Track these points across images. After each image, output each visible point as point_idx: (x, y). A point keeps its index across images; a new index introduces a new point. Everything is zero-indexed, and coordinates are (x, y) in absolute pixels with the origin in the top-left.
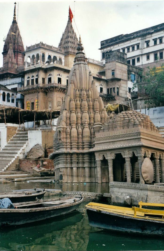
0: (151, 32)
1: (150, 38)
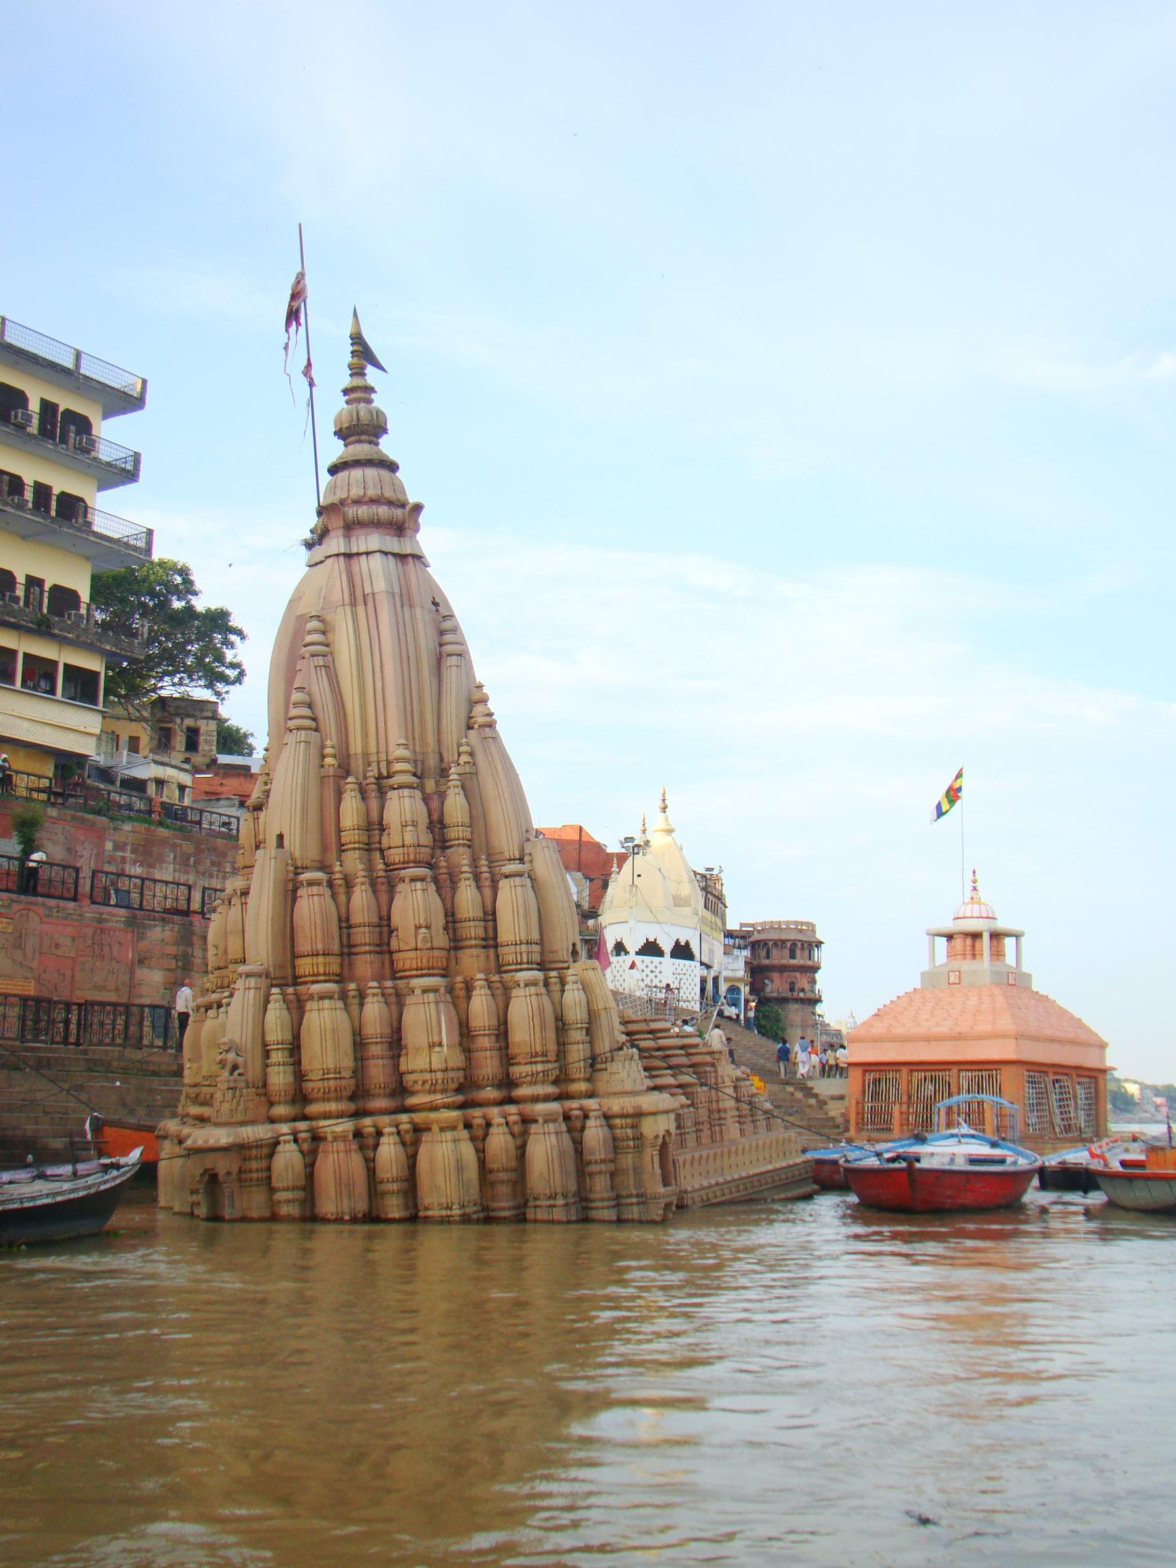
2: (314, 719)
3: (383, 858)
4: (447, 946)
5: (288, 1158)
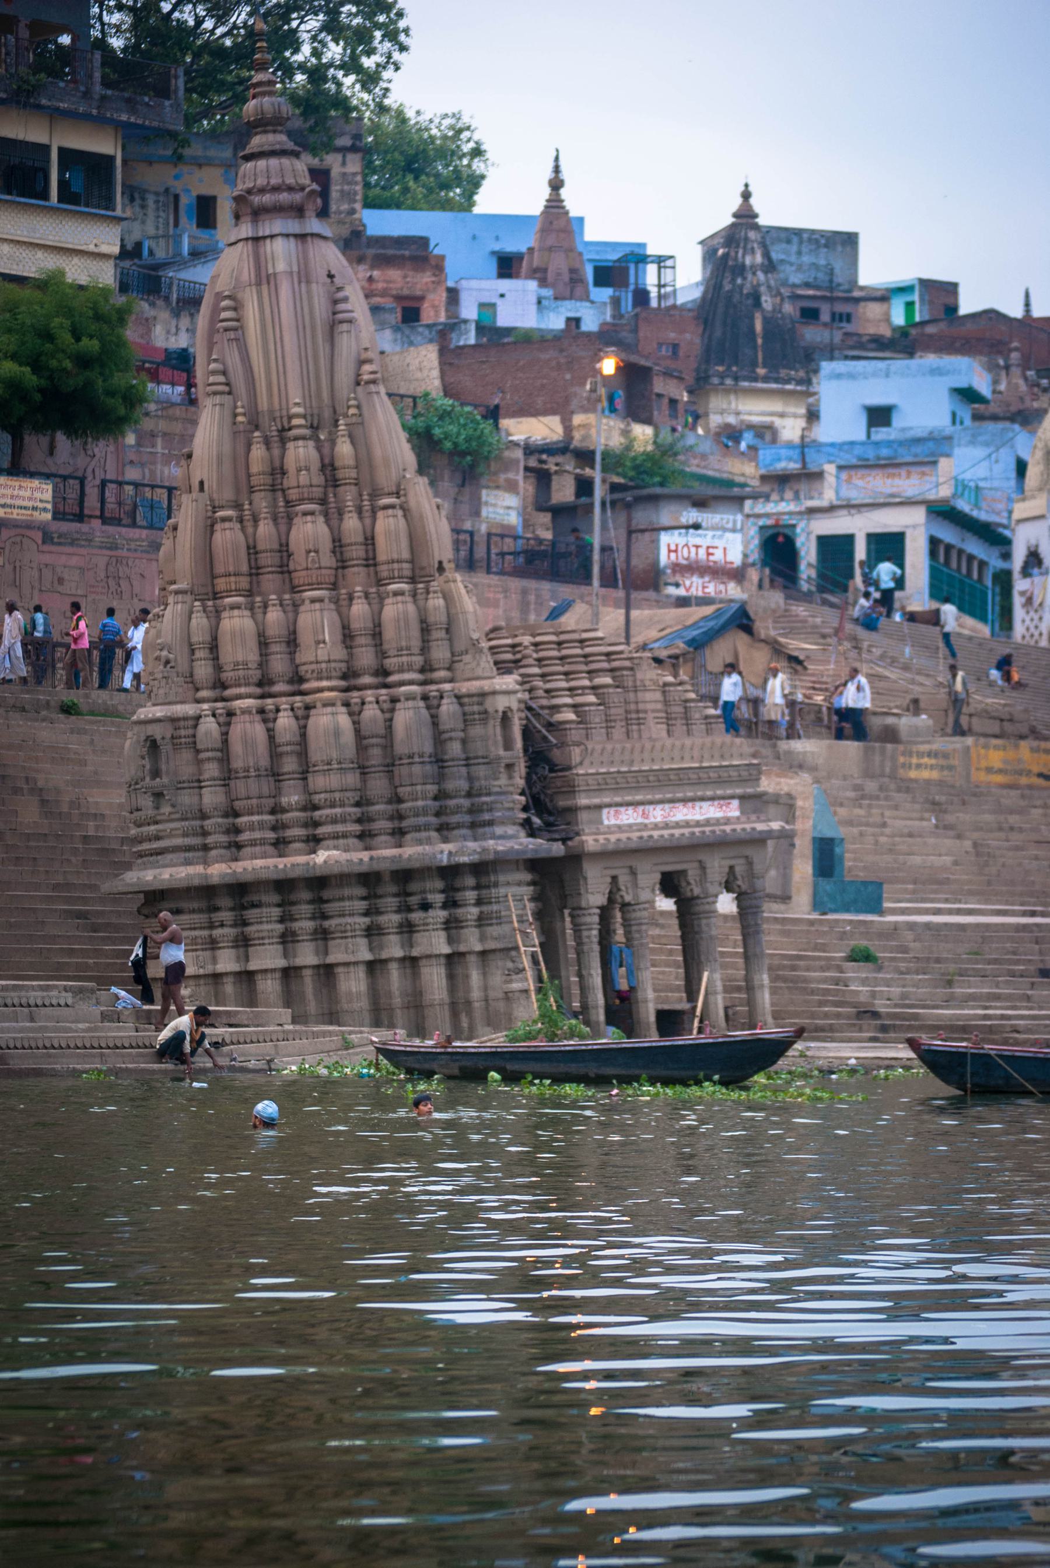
2: (227, 384)
3: (285, 497)
4: (334, 565)
5: (209, 726)
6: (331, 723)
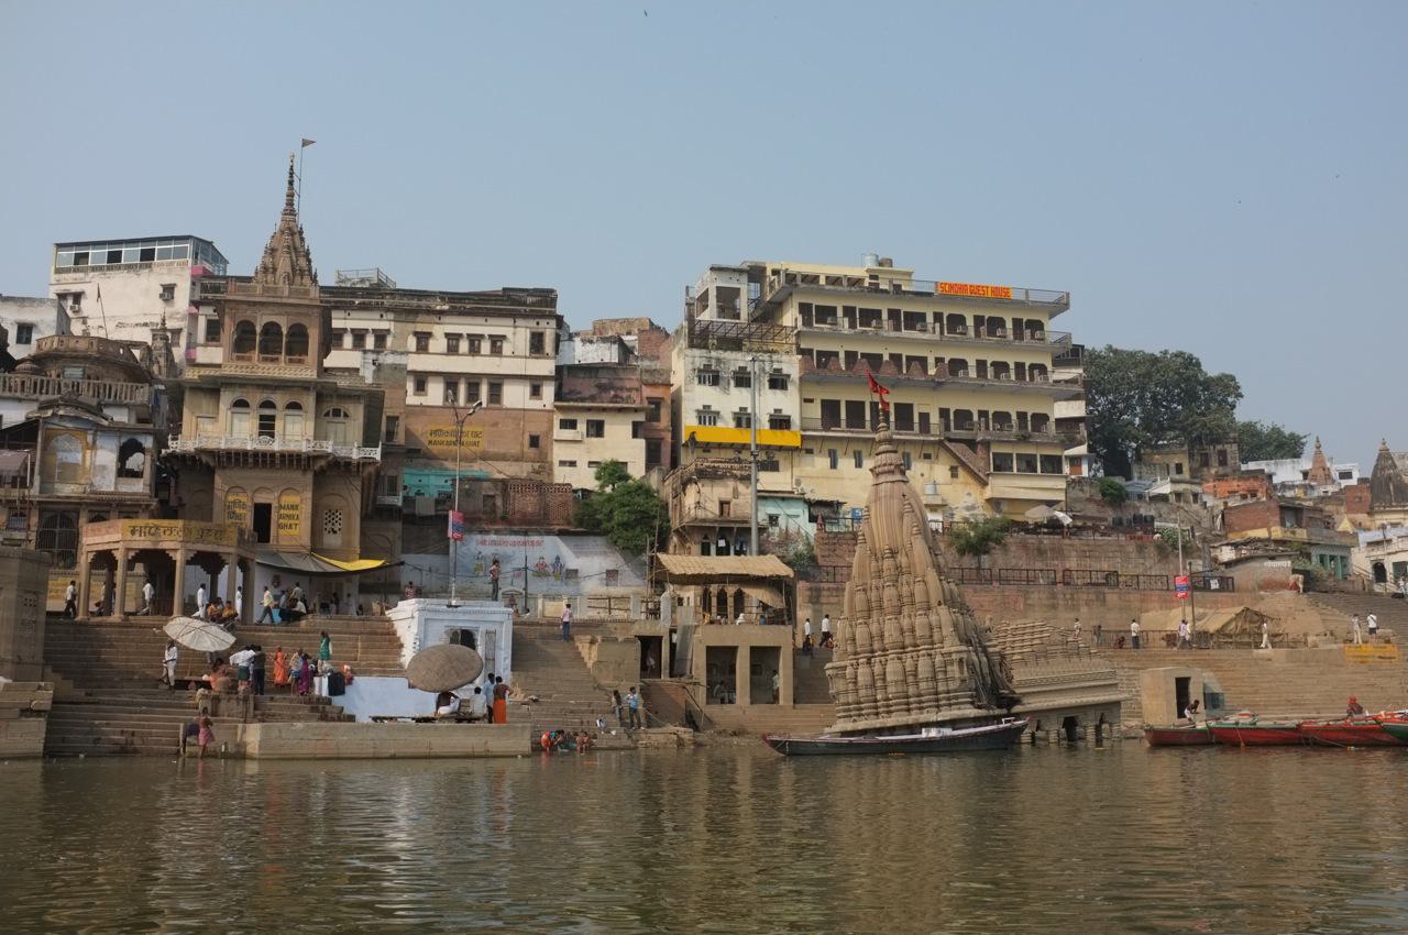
0: (438, 308)
1: (439, 331)
6: (892, 668)
